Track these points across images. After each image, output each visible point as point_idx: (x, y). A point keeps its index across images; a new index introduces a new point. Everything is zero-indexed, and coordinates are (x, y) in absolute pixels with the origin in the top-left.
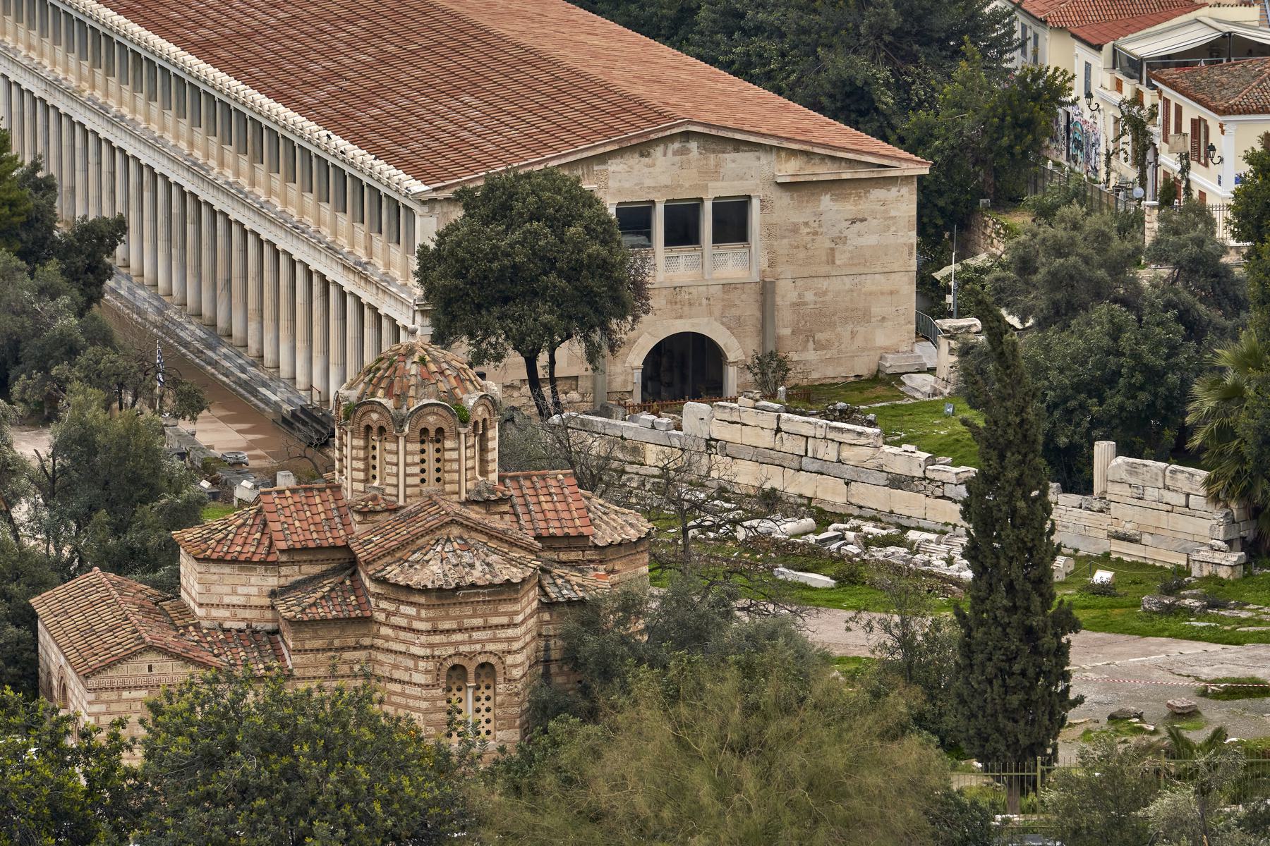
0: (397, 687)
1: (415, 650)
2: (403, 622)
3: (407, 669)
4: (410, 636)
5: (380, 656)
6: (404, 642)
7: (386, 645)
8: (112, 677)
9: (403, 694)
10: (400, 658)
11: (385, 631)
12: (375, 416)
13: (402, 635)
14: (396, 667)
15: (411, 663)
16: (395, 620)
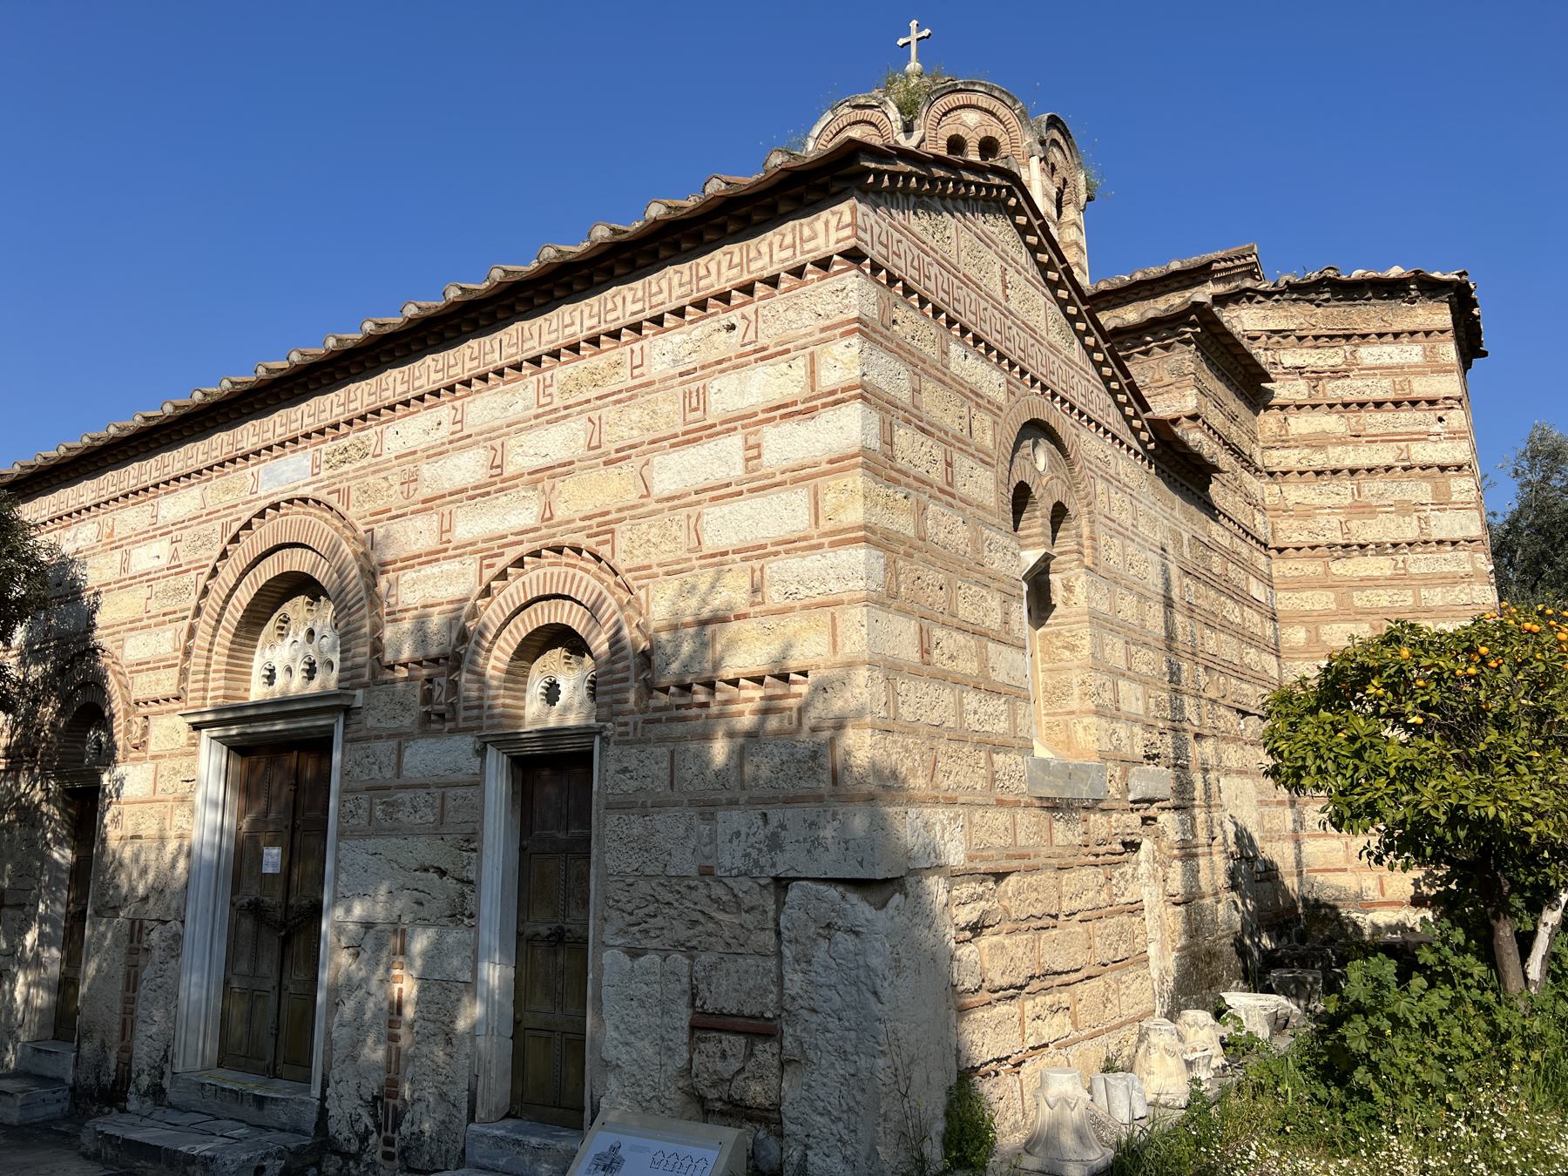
0: (1377, 566)
1: (1423, 453)
2: (1381, 389)
3: (1405, 509)
4: (1406, 419)
5: (1295, 493)
6: (1387, 438)
7: (1318, 461)
8: (920, 243)
9: (1400, 579)
10: (1376, 485)
11: (1301, 424)
12: (971, 117)
13: (1375, 421)
14: (1363, 509)
15: (1421, 491)
16: (1336, 390)
